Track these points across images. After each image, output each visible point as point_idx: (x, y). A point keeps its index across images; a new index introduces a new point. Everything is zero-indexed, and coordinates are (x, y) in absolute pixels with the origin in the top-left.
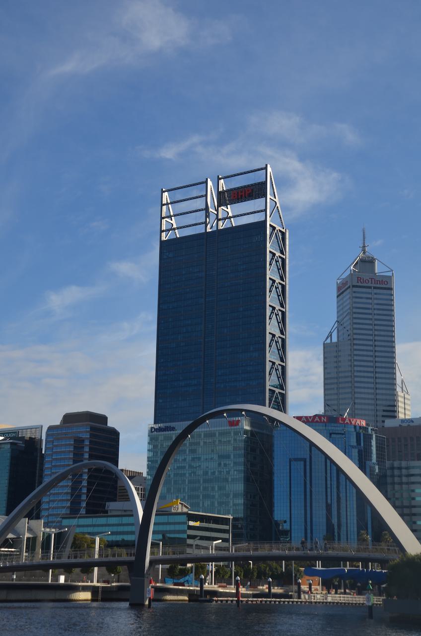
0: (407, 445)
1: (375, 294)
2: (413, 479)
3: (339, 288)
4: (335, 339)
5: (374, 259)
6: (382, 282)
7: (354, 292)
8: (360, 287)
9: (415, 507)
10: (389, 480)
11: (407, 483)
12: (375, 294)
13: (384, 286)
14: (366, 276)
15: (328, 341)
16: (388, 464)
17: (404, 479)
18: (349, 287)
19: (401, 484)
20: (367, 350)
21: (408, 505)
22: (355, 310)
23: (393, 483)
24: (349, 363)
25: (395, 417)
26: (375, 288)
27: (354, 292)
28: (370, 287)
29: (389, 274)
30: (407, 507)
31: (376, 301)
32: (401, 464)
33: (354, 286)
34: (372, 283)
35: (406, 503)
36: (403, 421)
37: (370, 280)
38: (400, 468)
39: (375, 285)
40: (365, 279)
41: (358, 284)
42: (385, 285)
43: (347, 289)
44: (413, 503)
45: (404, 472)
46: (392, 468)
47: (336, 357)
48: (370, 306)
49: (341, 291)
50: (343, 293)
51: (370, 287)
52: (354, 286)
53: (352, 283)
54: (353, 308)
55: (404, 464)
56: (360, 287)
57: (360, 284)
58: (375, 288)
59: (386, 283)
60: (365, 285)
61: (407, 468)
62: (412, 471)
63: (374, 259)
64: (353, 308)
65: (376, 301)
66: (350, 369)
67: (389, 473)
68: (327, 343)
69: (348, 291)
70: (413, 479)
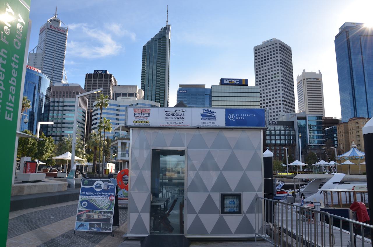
0: (64, 96)
1: (58, 35)
2: (65, 108)
3: (41, 31)
4: (35, 52)
5: (60, 21)
6: (62, 31)
7: (48, 31)
8: (51, 30)
9: (64, 123)
10: (51, 108)
11: (61, 111)
12: (58, 35)
13: (62, 32)
14: (55, 26)
15: (32, 52)
16: (52, 99)
17: (60, 108)
18: (46, 29)
19: (58, 110)
20: (51, 55)
21: (61, 122)
22: (47, 40)
23: (53, 110)
24: (41, 64)
25: (61, 82)
26: (58, 32)
27: (48, 31)
28: (56, 32)
29: (66, 28)
30: (60, 123)
31: (58, 38)
32: (59, 100)
33: (48, 29)
34: (57, 30)
35: (59, 121)
36: (63, 84)
37: (56, 28)
38: (58, 102)
39: (59, 31)
40: (54, 27)
41: (50, 28)
42: (63, 33)
43: (45, 29)
44: (64, 121)
45: (61, 104)
46: (54, 102)
47: (35, 60)
48: (55, 40)
49: (42, 32)
50: (42, 32)
51: (56, 32)
52: (48, 29)
53: (47, 27)
54: (46, 38)
55: (61, 100)
56: (51, 30)
57: (51, 29)
58: (58, 32)
59: (64, 31)
60: (54, 29)
61: (63, 102)
62: (65, 104)
63: (60, 21)
64: (47, 34)
65: (58, 38)
66: (41, 66)
67: (52, 104)
68: (31, 53)
69: (45, 30)
70: (65, 108)
